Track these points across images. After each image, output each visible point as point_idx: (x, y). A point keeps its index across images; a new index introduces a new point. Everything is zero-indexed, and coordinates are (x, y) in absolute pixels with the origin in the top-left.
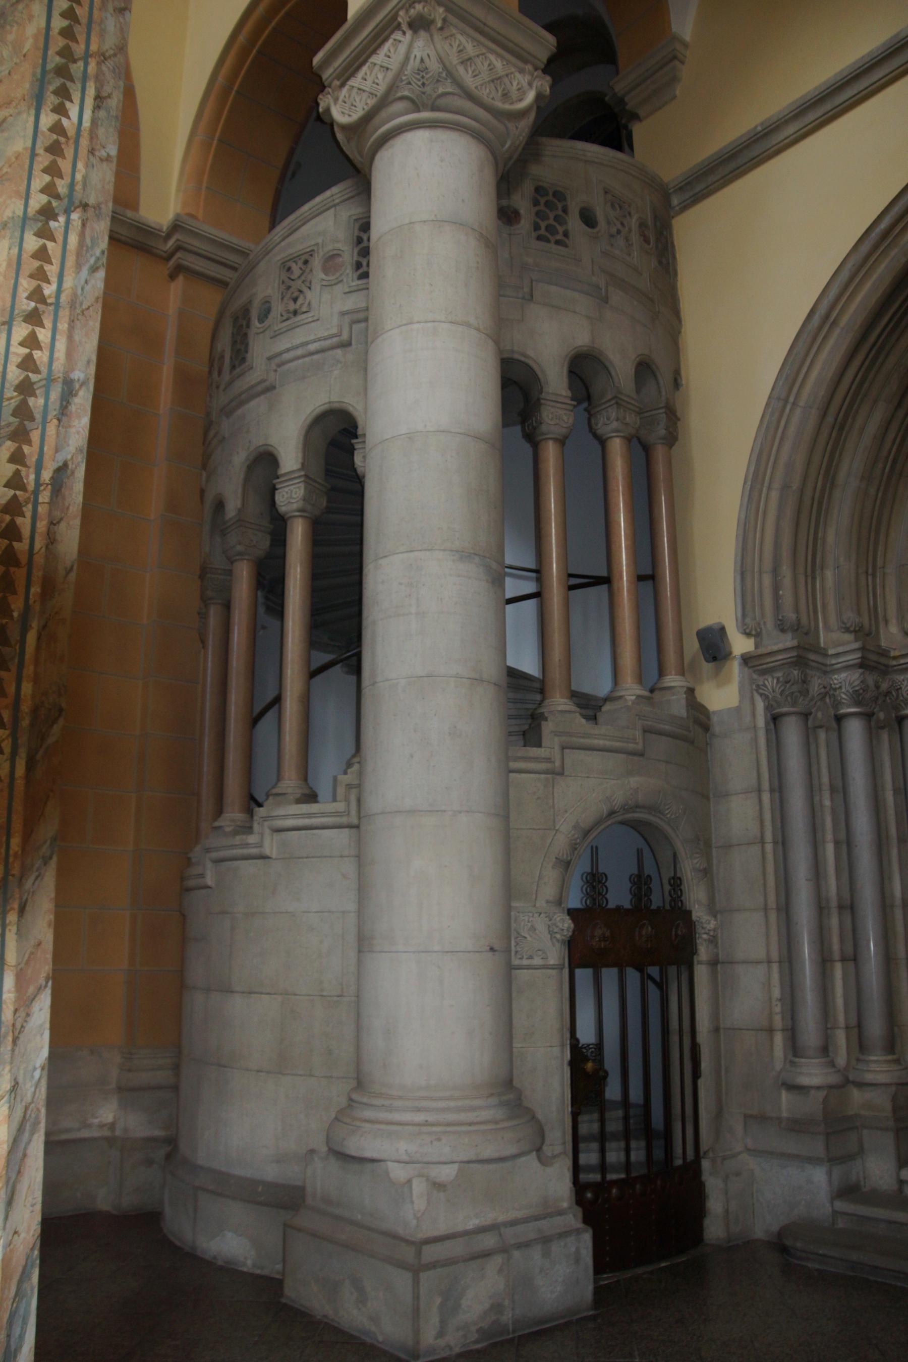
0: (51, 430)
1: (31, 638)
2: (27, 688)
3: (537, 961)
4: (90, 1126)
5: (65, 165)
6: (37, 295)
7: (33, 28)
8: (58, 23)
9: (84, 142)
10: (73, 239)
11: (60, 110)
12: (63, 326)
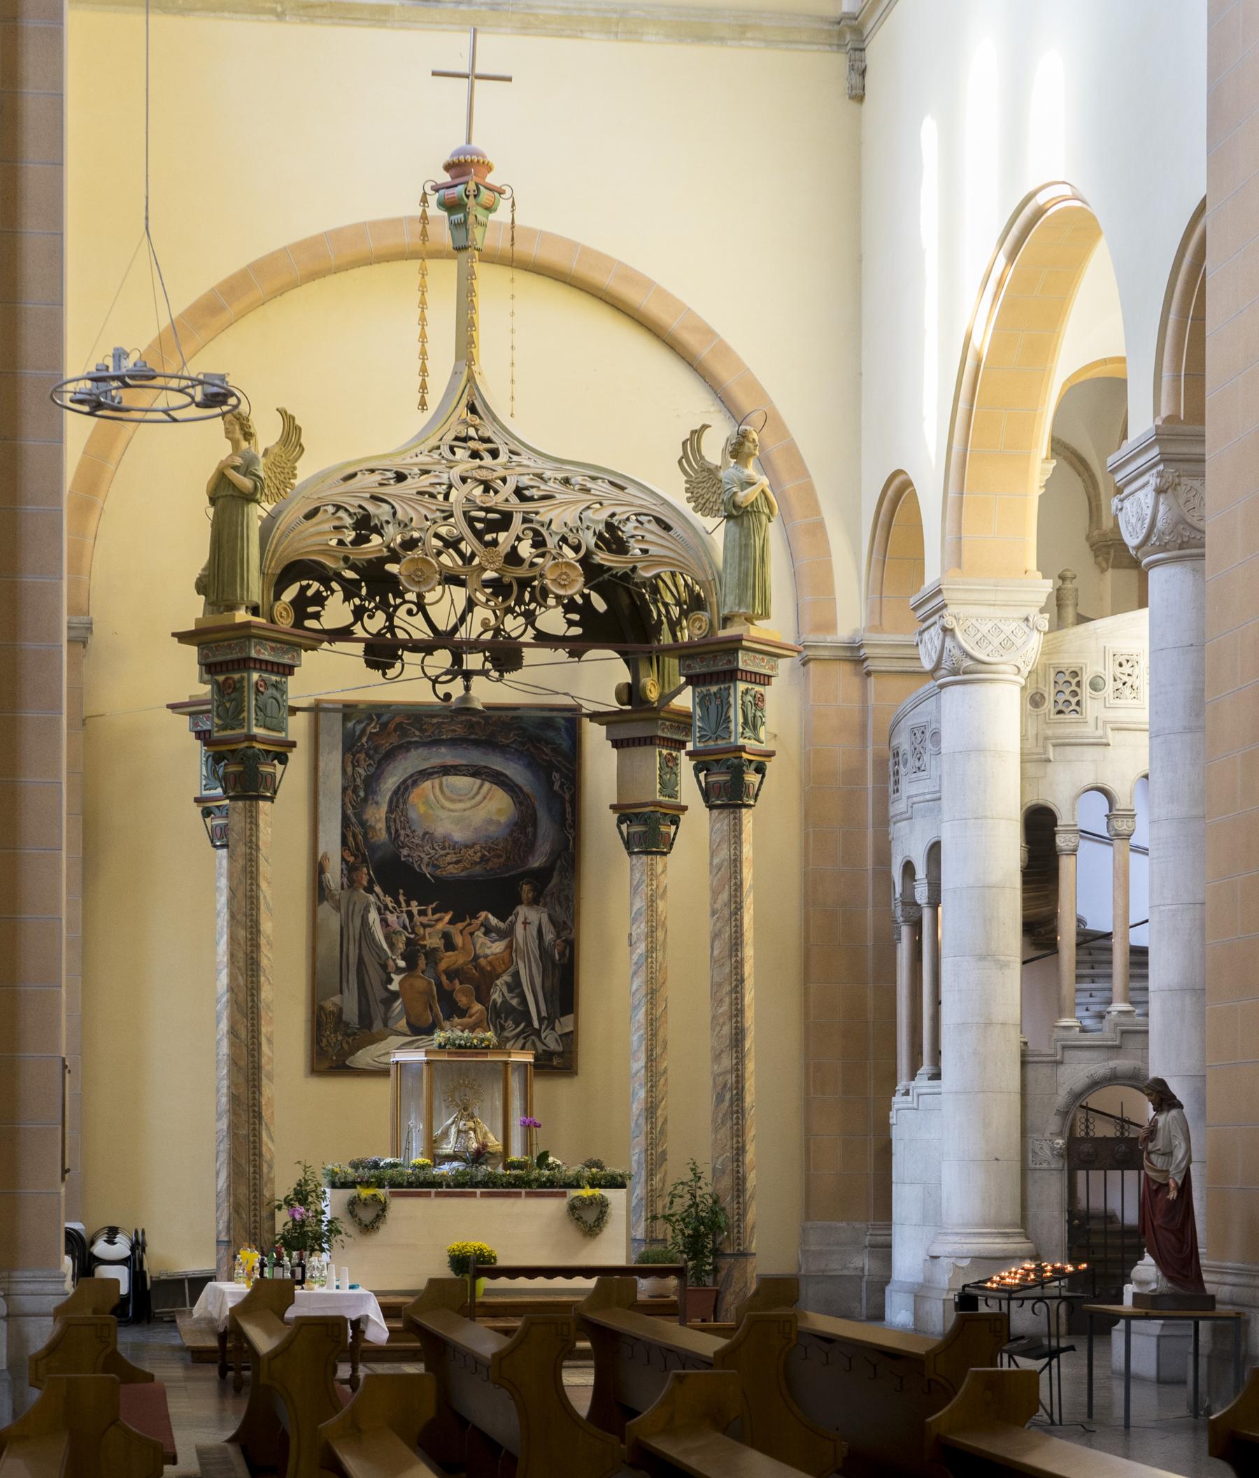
3: (1045, 1166)
4: (848, 1268)
7: (727, 935)
8: (733, 930)
11: (737, 955)
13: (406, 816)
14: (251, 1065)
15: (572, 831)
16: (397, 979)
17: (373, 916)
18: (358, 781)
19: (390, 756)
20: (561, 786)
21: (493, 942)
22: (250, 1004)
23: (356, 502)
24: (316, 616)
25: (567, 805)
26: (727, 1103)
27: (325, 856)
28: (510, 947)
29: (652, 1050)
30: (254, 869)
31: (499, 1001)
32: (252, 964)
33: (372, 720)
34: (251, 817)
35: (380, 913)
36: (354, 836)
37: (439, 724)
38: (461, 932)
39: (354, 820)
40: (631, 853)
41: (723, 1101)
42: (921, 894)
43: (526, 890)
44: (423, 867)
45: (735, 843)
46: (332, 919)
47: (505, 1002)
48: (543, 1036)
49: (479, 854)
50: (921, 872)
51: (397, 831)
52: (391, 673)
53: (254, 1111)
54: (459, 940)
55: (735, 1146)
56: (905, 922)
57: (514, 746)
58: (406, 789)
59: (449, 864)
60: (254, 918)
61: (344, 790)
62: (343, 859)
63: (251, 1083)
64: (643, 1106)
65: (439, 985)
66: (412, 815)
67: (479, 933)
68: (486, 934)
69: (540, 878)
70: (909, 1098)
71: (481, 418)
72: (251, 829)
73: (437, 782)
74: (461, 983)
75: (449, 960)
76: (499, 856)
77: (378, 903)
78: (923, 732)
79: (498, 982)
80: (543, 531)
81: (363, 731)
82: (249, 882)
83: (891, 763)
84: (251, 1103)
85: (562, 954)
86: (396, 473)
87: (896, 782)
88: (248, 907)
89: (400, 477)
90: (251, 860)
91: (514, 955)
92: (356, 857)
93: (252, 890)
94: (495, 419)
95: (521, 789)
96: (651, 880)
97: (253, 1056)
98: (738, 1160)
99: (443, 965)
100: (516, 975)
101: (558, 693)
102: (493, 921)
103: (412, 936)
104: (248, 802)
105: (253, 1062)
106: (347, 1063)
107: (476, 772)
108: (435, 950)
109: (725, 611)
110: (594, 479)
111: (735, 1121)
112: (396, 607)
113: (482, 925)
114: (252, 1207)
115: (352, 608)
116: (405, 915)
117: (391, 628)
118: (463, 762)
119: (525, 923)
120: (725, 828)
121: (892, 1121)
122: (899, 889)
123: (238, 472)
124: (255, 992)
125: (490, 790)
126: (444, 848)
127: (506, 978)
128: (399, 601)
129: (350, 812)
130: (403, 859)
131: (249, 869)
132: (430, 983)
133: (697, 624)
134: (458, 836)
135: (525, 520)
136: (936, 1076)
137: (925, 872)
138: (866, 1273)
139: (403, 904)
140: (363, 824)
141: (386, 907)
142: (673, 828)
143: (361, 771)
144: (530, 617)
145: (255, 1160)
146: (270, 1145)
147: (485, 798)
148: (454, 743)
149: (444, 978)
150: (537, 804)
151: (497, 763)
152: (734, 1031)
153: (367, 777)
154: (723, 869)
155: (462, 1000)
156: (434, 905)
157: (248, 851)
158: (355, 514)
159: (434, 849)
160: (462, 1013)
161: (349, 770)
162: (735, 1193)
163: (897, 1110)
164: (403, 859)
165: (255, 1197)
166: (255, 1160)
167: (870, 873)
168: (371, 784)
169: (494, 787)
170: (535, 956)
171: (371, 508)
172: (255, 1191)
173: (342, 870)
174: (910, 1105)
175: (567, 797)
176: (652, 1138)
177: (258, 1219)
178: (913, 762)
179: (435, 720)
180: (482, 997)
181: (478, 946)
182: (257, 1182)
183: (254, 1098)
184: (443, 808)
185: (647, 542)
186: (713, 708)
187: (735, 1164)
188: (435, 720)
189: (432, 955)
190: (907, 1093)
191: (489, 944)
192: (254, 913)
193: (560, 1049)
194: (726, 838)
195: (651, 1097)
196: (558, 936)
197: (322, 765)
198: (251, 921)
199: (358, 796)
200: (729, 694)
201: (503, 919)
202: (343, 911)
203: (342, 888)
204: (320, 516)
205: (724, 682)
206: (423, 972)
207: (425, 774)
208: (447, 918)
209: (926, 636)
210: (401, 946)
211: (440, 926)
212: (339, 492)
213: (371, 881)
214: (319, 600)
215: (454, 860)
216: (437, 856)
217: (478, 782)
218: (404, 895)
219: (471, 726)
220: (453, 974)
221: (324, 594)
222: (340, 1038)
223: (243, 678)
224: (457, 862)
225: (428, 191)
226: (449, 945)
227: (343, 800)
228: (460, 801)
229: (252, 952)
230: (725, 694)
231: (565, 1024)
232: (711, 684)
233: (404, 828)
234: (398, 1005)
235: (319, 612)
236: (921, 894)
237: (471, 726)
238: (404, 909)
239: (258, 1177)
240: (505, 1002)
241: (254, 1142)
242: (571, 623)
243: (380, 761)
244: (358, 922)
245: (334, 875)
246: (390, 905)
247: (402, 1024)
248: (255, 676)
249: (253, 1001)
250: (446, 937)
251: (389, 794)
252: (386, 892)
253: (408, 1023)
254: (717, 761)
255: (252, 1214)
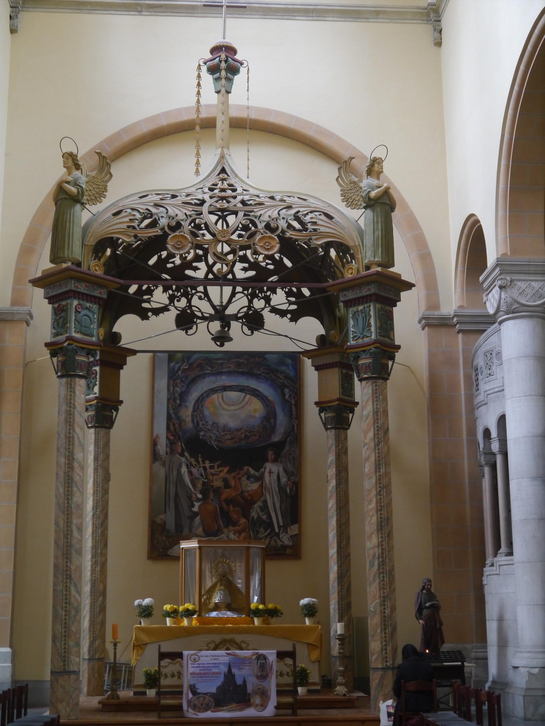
0: (386, 527)
1: (387, 560)
2: (387, 568)
5: (382, 481)
6: (381, 506)
7: (373, 459)
9: (384, 476)
10: (385, 494)
11: (380, 472)
12: (385, 510)
13: (203, 414)
14: (65, 544)
15: (296, 421)
16: (197, 504)
17: (184, 469)
18: (176, 395)
19: (194, 381)
20: (290, 396)
21: (252, 483)
22: (66, 505)
23: (145, 207)
24: (148, 301)
25: (294, 408)
26: (376, 567)
27: (157, 436)
28: (261, 486)
29: (341, 542)
30: (72, 420)
31: (256, 516)
32: (68, 479)
33: (184, 362)
34: (71, 387)
35: (188, 467)
36: (174, 425)
37: (222, 364)
38: (234, 478)
39: (173, 416)
40: (327, 429)
41: (373, 565)
42: (495, 446)
43: (270, 454)
44: (212, 442)
45: (377, 401)
46: (161, 472)
47: (259, 517)
48: (281, 536)
49: (244, 434)
50: (494, 434)
51: (197, 422)
52: (190, 332)
53: (67, 574)
54: (232, 483)
55: (382, 595)
56: (485, 464)
57: (263, 375)
58: (203, 399)
59: (227, 440)
60: (71, 450)
61: (169, 400)
62: (167, 438)
63: (65, 556)
64: (336, 575)
65: (221, 508)
66: (206, 413)
67: (244, 479)
68: (248, 479)
69: (278, 447)
70: (494, 568)
71: (228, 175)
72: (71, 395)
73: (220, 395)
74: (234, 507)
75: (227, 493)
76: (255, 435)
77: (187, 462)
78: (491, 354)
79: (255, 506)
80: (256, 220)
81: (179, 369)
82: (68, 428)
83: (474, 376)
84: (65, 569)
85: (291, 490)
86: (172, 195)
87: (477, 385)
88: (67, 444)
89: (174, 196)
90: (70, 414)
91: (264, 491)
92: (175, 436)
93: (70, 433)
94: (236, 176)
95: (267, 398)
96: (338, 443)
97: (67, 538)
98: (384, 605)
99: (223, 497)
100: (265, 502)
101: (280, 335)
102: (252, 471)
103: (206, 480)
104: (69, 379)
105: (67, 542)
106: (168, 553)
107: (242, 389)
108: (219, 488)
109: (366, 261)
110: (289, 196)
111: (381, 579)
112: (193, 295)
113: (246, 474)
114: (63, 639)
115: (168, 296)
116: (202, 469)
117: (190, 306)
118: (235, 384)
119: (270, 472)
120: (370, 391)
121: (484, 583)
122: (482, 446)
123: (69, 185)
124: (69, 497)
125: (249, 400)
126: (224, 431)
127: (259, 503)
128: (194, 291)
129: (171, 412)
130: (201, 437)
131: (68, 420)
132: (216, 507)
133: (350, 271)
134: (232, 424)
135: (245, 215)
136: (510, 554)
137: (497, 433)
138: (473, 675)
139: (201, 463)
140: (178, 418)
141: (191, 464)
142: (351, 415)
143: (178, 389)
144: (268, 300)
145: (66, 607)
146: (77, 597)
147: (247, 403)
148: (230, 373)
149: (224, 505)
150: (276, 406)
151: (253, 384)
152: (379, 520)
153: (181, 393)
154: (369, 418)
155: (234, 516)
156: (218, 463)
157: (68, 409)
158: (143, 213)
159: (218, 432)
160: (235, 524)
161: (171, 389)
162: (383, 627)
163: (487, 576)
164: (201, 437)
165: (65, 631)
166: (66, 607)
167: (465, 441)
168: (183, 396)
169: (252, 397)
170: (276, 492)
171: (154, 210)
172: (65, 627)
173: (167, 444)
174: (495, 572)
175: (293, 402)
176: (342, 595)
177: (67, 646)
178: (486, 372)
179: (219, 362)
180: (246, 515)
181: (243, 485)
182: (67, 621)
183: (67, 566)
184: (224, 409)
185: (318, 225)
186: (360, 319)
187: (383, 607)
188: (219, 362)
189: (217, 491)
190: (492, 565)
191: (250, 484)
192: (71, 447)
193: (291, 544)
194: (371, 398)
195: (341, 570)
196: (289, 480)
197: (156, 386)
198: (69, 452)
199: (176, 403)
200: (370, 310)
201: (258, 471)
202: (167, 466)
203: (167, 453)
204: (123, 214)
205: (366, 303)
206: (212, 501)
207: (214, 391)
208: (226, 470)
209: (490, 295)
210: (200, 486)
211: (222, 475)
212: (134, 202)
213: (183, 451)
214: (150, 292)
215: (230, 437)
216: (220, 436)
217: (243, 394)
218: (201, 457)
219: (239, 365)
220: (228, 502)
221: (152, 288)
222: (164, 539)
223: (68, 304)
224: (231, 439)
225: (202, 64)
226: (227, 485)
227: (168, 405)
228: (233, 405)
229: (69, 471)
230: (367, 309)
231: (294, 530)
232: (358, 305)
233: (202, 421)
234: (197, 520)
235: (150, 298)
236: (495, 446)
237: (239, 365)
238: (202, 465)
239: (68, 618)
240: (259, 517)
241: (66, 595)
242: (291, 303)
243: (188, 385)
244: (175, 473)
245: (162, 447)
246: (194, 463)
247: (200, 531)
248: (75, 302)
249: (68, 503)
250: (225, 480)
251: (193, 402)
252: (191, 456)
253: (204, 530)
254: (364, 351)
255: (63, 643)
